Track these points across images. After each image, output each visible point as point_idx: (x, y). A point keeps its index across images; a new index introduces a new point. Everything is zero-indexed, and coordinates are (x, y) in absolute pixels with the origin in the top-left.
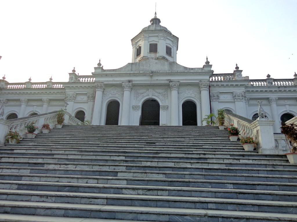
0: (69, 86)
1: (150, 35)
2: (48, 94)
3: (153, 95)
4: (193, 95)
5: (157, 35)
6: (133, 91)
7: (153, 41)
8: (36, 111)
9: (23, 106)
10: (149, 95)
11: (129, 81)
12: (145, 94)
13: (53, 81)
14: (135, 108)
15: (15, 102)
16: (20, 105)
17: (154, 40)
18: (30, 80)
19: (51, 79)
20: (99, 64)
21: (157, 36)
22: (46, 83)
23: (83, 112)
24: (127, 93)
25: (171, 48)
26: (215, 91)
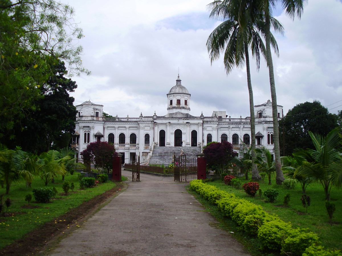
4: (196, 128)
6: (171, 126)
9: (117, 130)
11: (170, 123)
12: (175, 128)
13: (129, 117)
14: (172, 133)
16: (115, 130)
17: (178, 97)
18: (117, 116)
20: (155, 114)
22: (126, 118)
23: (149, 135)
24: (168, 128)
25: (187, 101)
26: (205, 125)
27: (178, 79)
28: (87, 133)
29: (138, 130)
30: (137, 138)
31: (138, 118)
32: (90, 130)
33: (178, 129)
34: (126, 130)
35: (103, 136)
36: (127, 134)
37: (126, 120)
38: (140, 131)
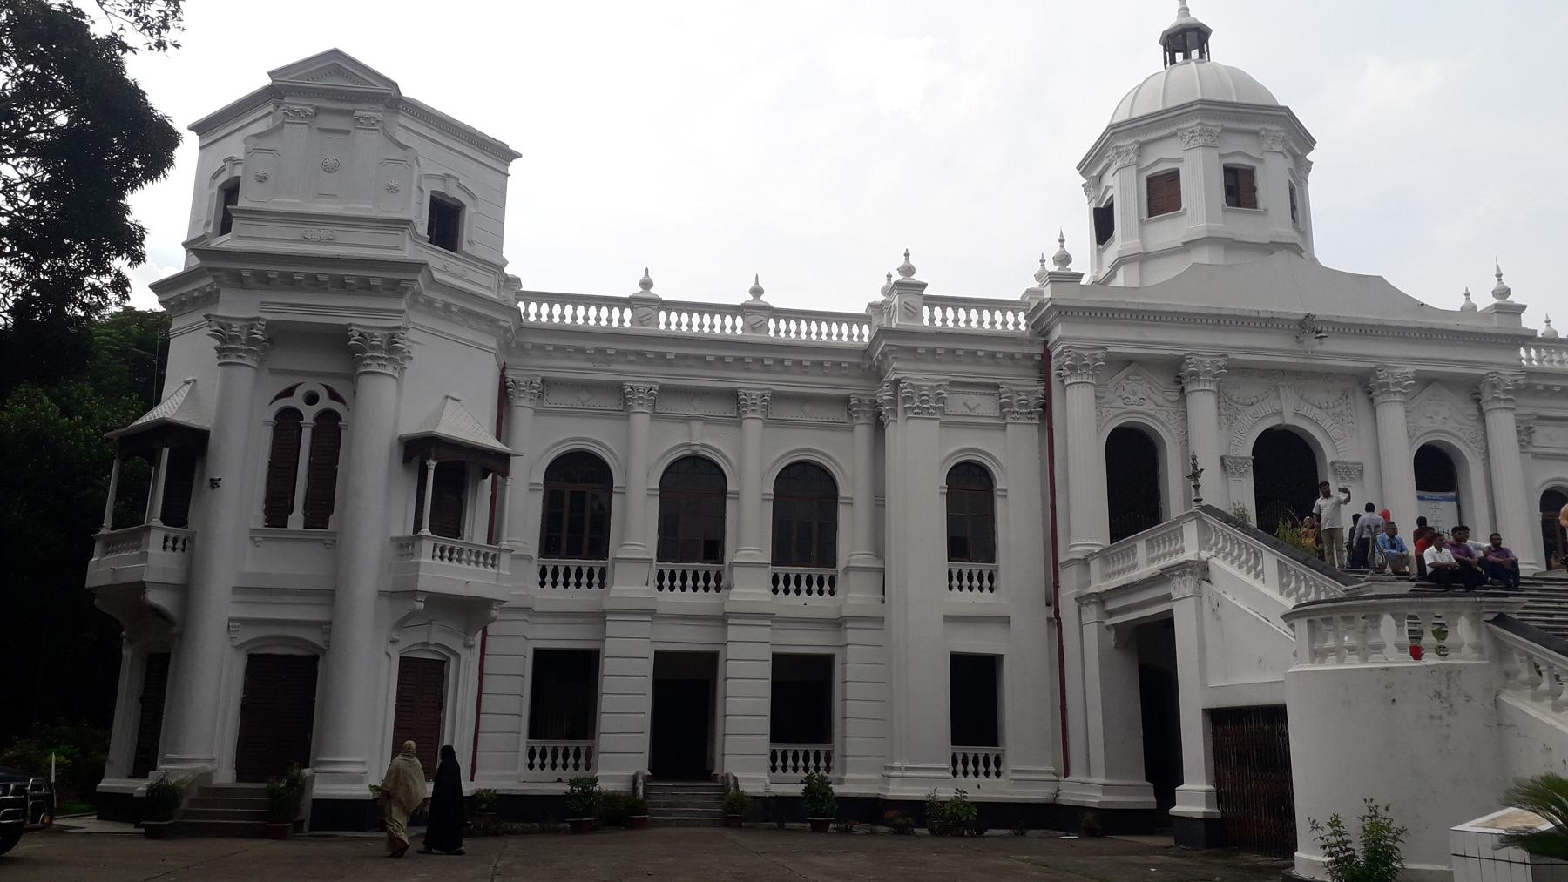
0: (915, 349)
1: (1228, 125)
2: (767, 369)
3: (1296, 414)
5: (1256, 127)
7: (1239, 153)
8: (703, 445)
9: (641, 421)
10: (1281, 413)
15: (584, 396)
16: (624, 413)
17: (1240, 150)
18: (646, 284)
19: (757, 292)
21: (1256, 133)
24: (1203, 405)
27: (1184, 20)
28: (309, 414)
29: (862, 432)
30: (843, 512)
31: (850, 318)
32: (352, 378)
33: (1289, 420)
34: (737, 420)
35: (496, 464)
36: (752, 462)
37: (734, 327)
38: (890, 431)
